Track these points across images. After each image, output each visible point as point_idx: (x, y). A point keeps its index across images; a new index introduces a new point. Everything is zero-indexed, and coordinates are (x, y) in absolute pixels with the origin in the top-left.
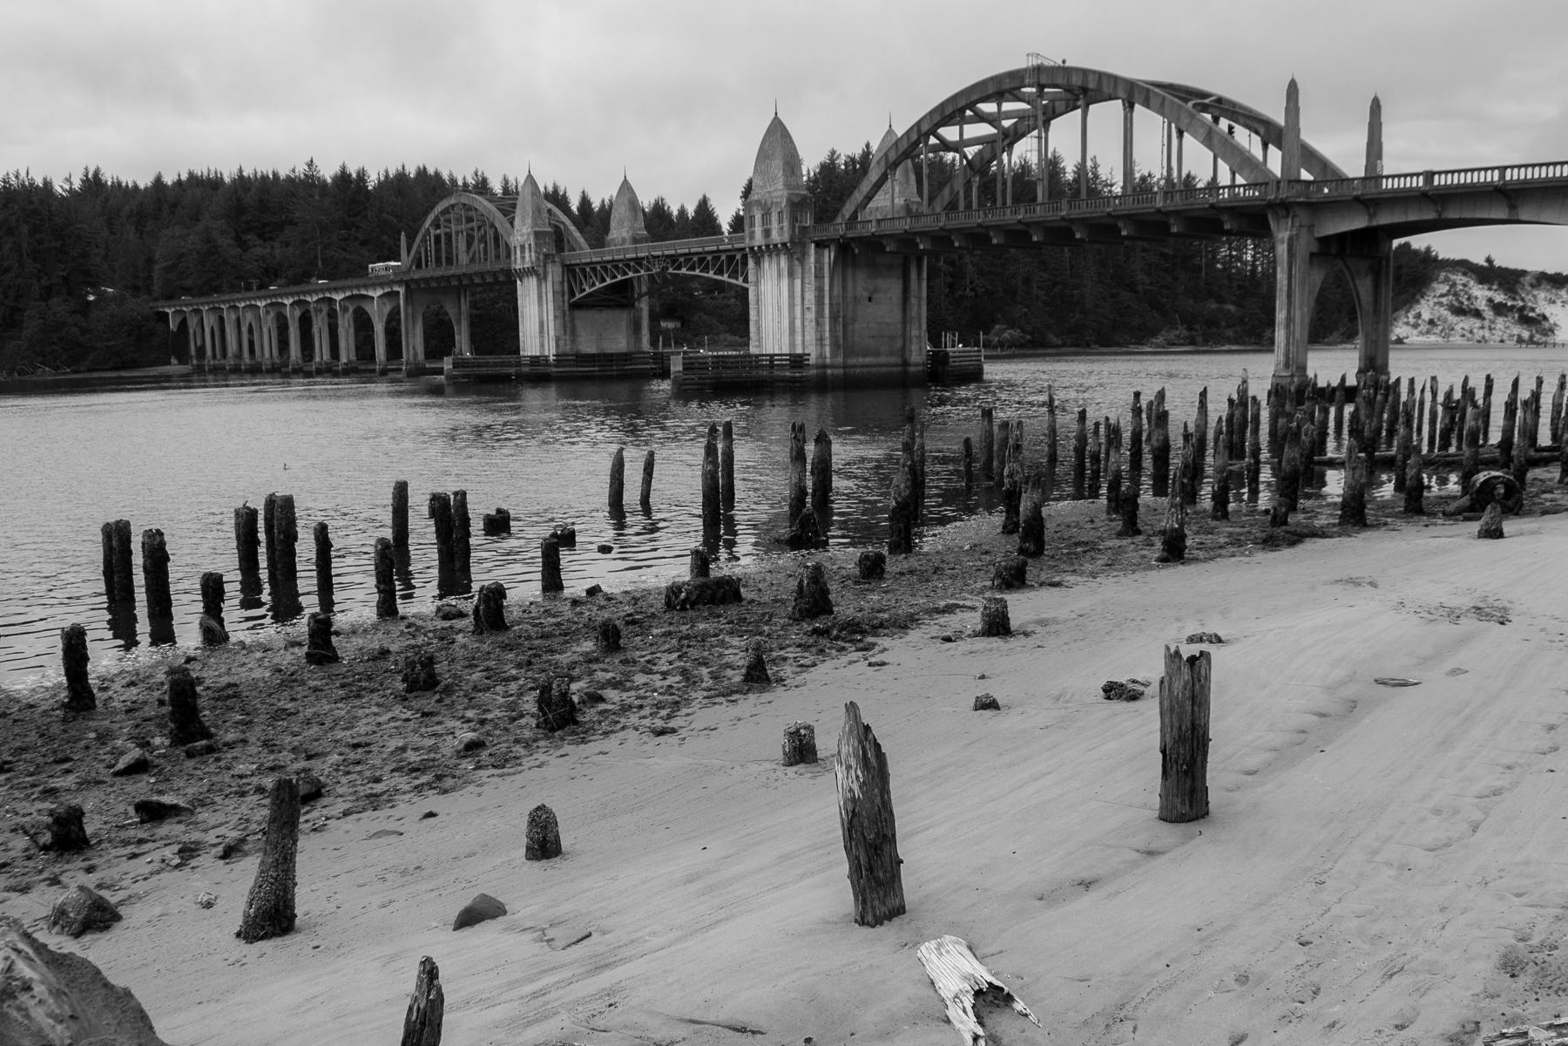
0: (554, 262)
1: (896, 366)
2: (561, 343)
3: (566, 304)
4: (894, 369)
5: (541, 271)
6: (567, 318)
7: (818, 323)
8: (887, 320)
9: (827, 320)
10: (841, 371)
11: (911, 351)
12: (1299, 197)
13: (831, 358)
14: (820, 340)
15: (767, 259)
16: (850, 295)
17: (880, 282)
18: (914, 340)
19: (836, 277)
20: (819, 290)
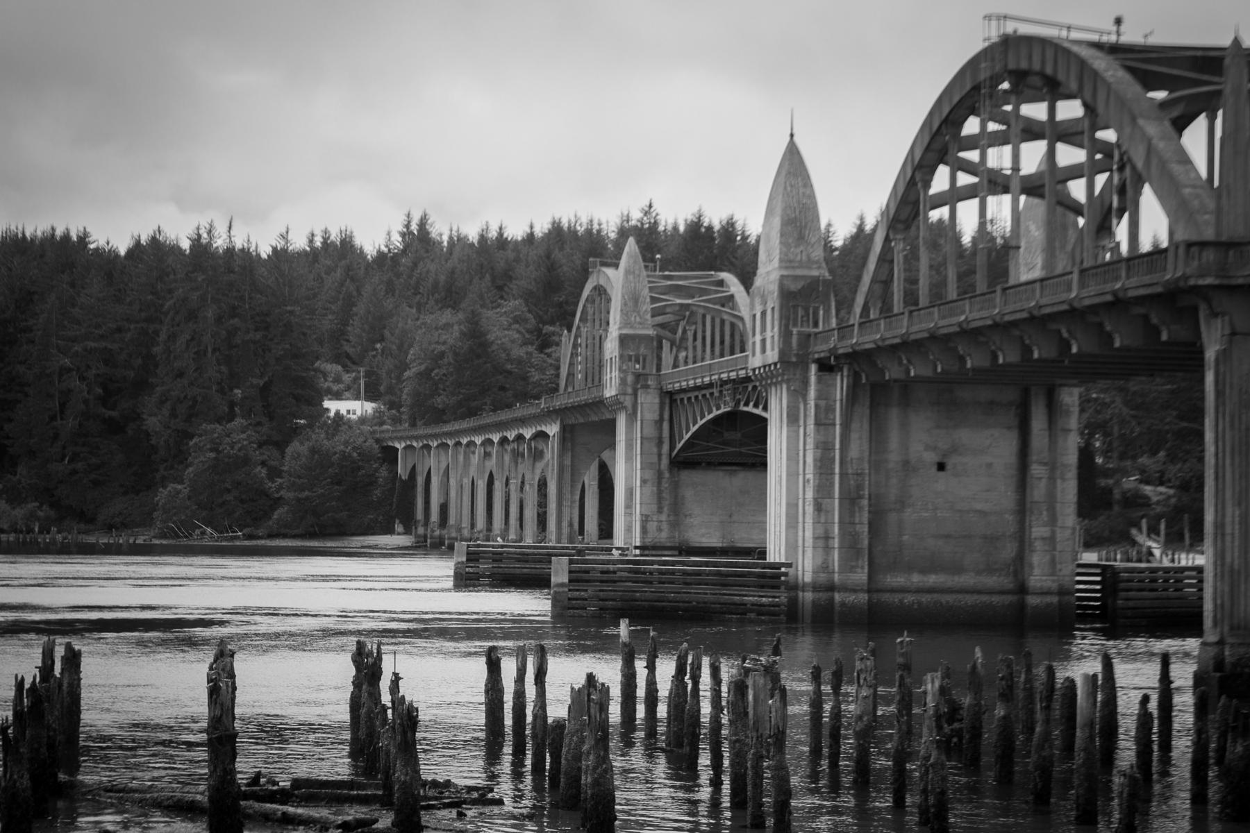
0: (646, 387)
1: (1002, 592)
2: (652, 526)
3: (665, 462)
4: (996, 599)
5: (628, 401)
6: (665, 485)
7: (818, 508)
8: (979, 506)
9: (837, 502)
10: (863, 597)
11: (1031, 566)
12: (1202, 276)
13: (840, 573)
14: (824, 539)
15: (773, 389)
16: (894, 457)
17: (965, 436)
18: (1038, 545)
19: (855, 425)
20: (824, 448)
